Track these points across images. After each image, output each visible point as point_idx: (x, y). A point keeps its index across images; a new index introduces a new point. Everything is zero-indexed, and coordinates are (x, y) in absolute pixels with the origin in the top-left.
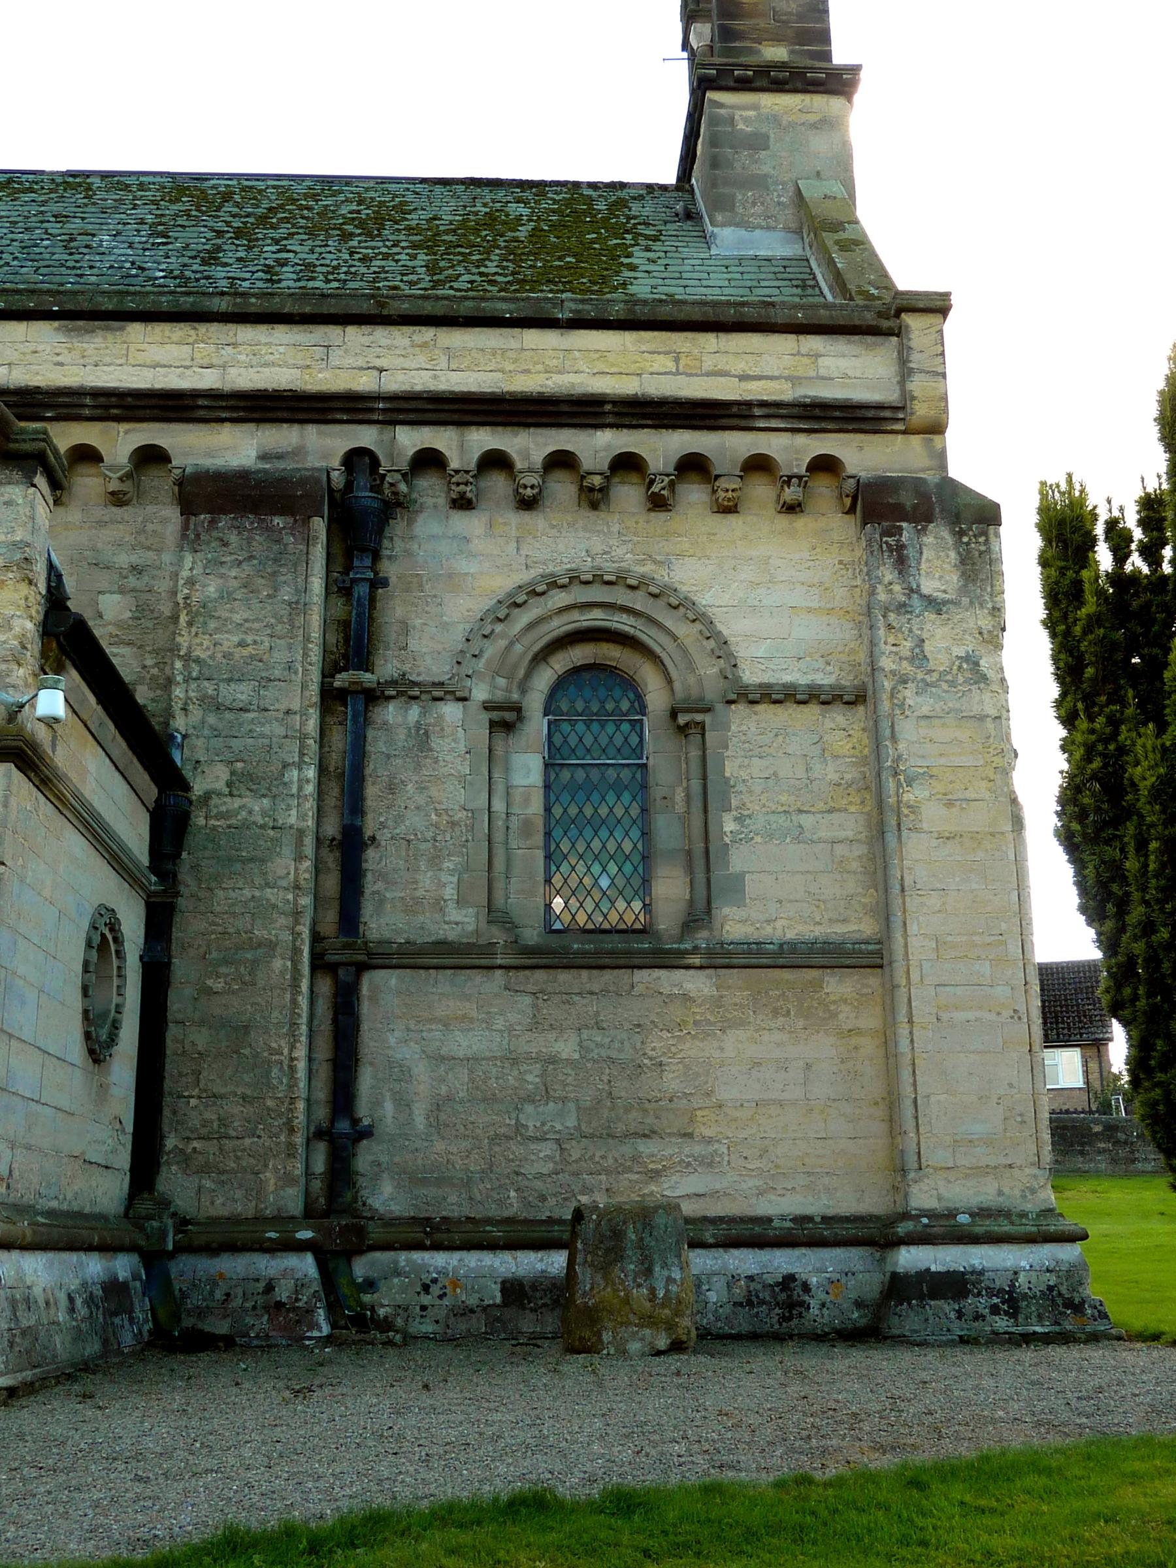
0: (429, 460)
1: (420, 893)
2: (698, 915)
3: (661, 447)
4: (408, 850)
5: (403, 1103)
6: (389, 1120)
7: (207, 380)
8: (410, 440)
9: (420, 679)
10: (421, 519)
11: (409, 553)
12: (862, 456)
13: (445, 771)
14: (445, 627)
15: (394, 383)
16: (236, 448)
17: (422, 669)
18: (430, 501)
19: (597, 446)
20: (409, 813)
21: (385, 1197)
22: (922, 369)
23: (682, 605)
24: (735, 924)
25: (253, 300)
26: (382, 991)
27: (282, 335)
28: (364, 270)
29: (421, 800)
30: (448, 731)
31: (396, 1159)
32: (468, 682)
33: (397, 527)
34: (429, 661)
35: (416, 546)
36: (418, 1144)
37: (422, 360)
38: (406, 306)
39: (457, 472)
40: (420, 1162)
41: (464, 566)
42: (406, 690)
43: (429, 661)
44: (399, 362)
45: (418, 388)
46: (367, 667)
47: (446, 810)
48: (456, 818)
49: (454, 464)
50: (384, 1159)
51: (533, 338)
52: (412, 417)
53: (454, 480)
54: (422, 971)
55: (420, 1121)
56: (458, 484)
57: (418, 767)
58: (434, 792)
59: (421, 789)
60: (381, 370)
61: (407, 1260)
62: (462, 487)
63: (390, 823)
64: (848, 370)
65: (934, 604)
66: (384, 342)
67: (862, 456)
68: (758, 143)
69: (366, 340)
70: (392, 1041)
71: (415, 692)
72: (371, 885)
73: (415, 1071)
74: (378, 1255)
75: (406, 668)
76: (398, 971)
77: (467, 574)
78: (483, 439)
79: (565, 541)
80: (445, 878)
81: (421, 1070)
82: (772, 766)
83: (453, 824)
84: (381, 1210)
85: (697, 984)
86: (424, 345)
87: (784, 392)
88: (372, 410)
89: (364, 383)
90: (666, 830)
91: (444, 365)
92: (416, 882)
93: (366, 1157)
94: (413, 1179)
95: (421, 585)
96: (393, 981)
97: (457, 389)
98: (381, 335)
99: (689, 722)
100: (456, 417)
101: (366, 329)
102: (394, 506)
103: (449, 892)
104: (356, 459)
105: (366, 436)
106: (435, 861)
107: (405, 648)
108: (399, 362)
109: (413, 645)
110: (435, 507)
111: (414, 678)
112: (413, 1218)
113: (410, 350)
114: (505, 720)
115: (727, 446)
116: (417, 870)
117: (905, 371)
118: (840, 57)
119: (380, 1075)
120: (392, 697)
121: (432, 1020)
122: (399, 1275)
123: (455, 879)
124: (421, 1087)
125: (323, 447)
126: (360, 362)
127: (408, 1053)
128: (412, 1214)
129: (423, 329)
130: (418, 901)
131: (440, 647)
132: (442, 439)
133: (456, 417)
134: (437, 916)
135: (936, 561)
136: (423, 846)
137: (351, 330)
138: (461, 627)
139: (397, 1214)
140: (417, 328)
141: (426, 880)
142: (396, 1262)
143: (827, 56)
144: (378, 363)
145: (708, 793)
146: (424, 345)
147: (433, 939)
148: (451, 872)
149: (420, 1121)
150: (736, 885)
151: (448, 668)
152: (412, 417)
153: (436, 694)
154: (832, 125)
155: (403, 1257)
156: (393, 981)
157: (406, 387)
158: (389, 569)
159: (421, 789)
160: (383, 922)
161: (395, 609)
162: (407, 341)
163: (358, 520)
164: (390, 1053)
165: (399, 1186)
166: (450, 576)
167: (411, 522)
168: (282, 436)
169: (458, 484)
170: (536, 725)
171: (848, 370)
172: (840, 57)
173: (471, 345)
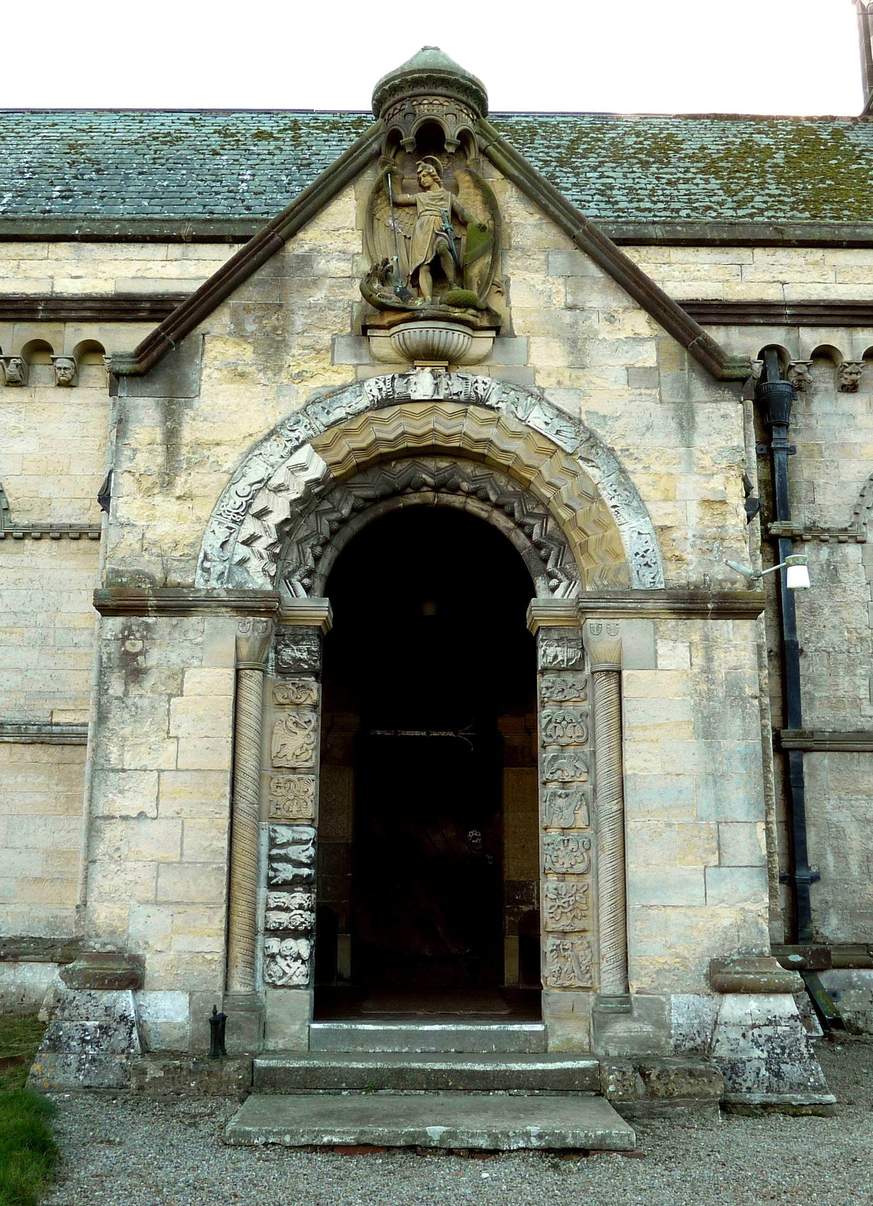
0: (825, 354)
1: (840, 693)
4: (829, 660)
5: (841, 855)
6: (832, 869)
8: (812, 338)
9: (827, 526)
10: (816, 400)
11: (809, 427)
13: (853, 598)
14: (842, 485)
15: (796, 293)
17: (827, 518)
18: (822, 386)
20: (827, 631)
25: (679, 228)
26: (819, 769)
27: (704, 255)
28: (675, 193)
29: (836, 620)
30: (852, 567)
31: (840, 898)
32: (864, 529)
33: (799, 406)
34: (833, 512)
35: (814, 422)
36: (855, 887)
37: (814, 275)
38: (798, 232)
39: (850, 364)
40: (857, 901)
41: (853, 437)
42: (818, 535)
43: (833, 512)
44: (798, 277)
45: (814, 298)
46: (787, 517)
47: (855, 629)
48: (864, 635)
49: (847, 358)
50: (829, 898)
52: (813, 320)
53: (847, 370)
54: (847, 754)
55: (855, 870)
56: (851, 374)
57: (831, 595)
58: (845, 614)
59: (835, 612)
60: (784, 283)
61: (859, 976)
62: (854, 377)
63: (813, 638)
66: (784, 261)
69: (771, 260)
70: (829, 807)
71: (826, 536)
72: (805, 687)
73: (848, 831)
74: (835, 971)
75: (816, 517)
76: (829, 753)
80: (859, 681)
81: (852, 829)
83: (862, 640)
84: (831, 937)
86: (816, 263)
88: (780, 315)
89: (772, 294)
91: (832, 279)
92: (837, 685)
93: (816, 896)
94: (852, 913)
95: (821, 453)
96: (826, 762)
97: (844, 298)
98: (782, 255)
100: (847, 321)
101: (770, 251)
103: (863, 693)
104: (772, 353)
105: (777, 336)
106: (850, 668)
107: (813, 502)
108: (798, 277)
109: (819, 499)
110: (826, 390)
111: (822, 525)
112: (855, 944)
113: (805, 267)
116: (837, 675)
119: (822, 834)
120: (808, 541)
121: (858, 792)
122: (854, 988)
123: (867, 683)
124: (854, 843)
126: (768, 277)
127: (842, 817)
128: (854, 941)
129: (814, 250)
130: (840, 700)
131: (840, 501)
133: (847, 321)
134: (856, 711)
136: (840, 657)
137: (758, 251)
138: (854, 485)
139: (843, 940)
140: (809, 250)
141: (845, 683)
142: (850, 978)
144: (781, 278)
146: (816, 263)
147: (854, 728)
148: (864, 677)
149: (855, 870)
151: (847, 518)
152: (813, 320)
153: (842, 538)
155: (855, 974)
156: (826, 762)
157: (805, 297)
158: (797, 440)
159: (835, 612)
160: (815, 716)
161: (803, 471)
162: (802, 261)
164: (828, 816)
165: (843, 919)
166: (843, 445)
167: (808, 403)
169: (851, 374)
173: (852, 263)
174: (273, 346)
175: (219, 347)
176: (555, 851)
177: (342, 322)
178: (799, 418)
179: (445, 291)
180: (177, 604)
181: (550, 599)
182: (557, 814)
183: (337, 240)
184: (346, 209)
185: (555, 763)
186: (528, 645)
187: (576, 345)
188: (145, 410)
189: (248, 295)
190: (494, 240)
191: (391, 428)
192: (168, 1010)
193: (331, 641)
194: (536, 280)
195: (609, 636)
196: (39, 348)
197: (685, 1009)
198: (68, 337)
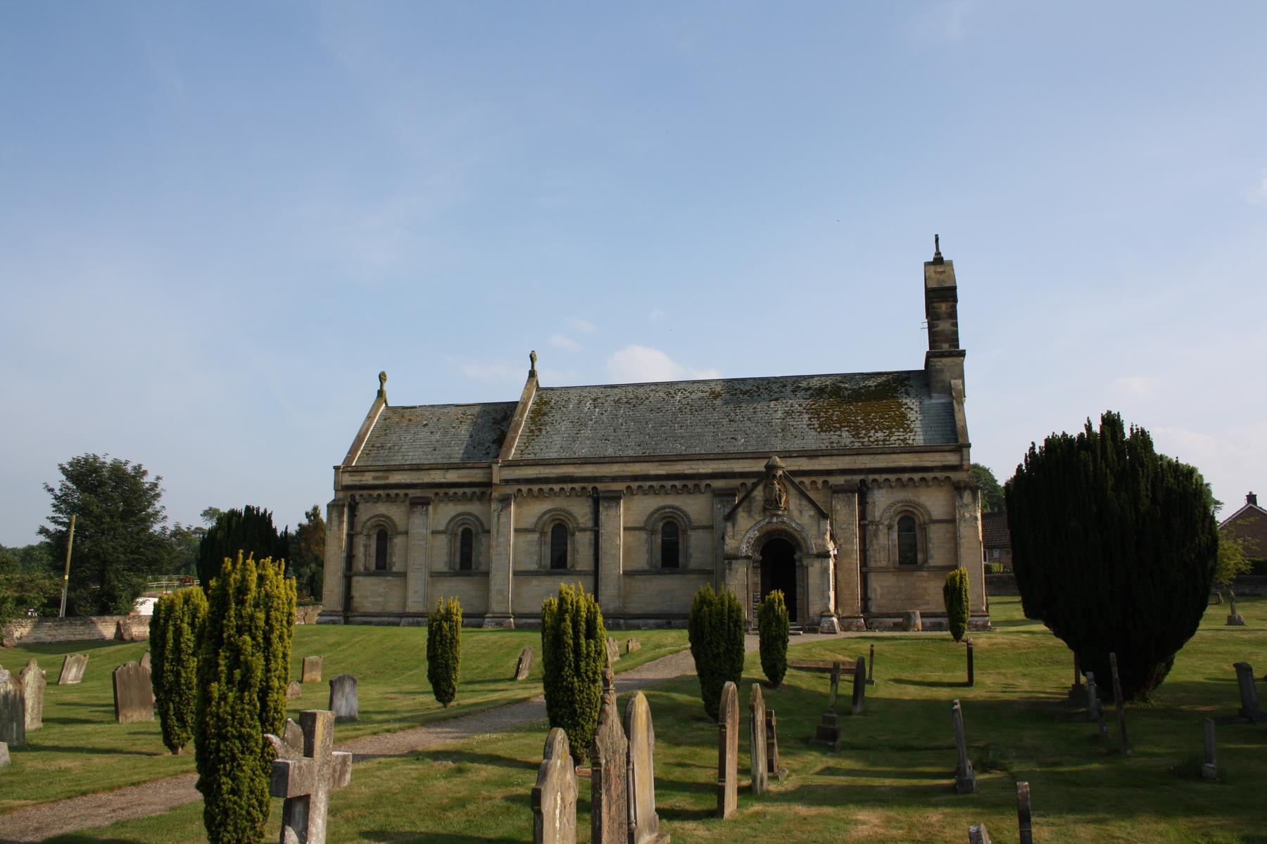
2: (926, 561)
7: (834, 467)
8: (871, 477)
12: (955, 476)
15: (868, 466)
16: (839, 480)
19: (905, 477)
21: (873, 609)
23: (922, 506)
24: (932, 562)
42: (872, 522)
51: (893, 456)
65: (966, 505)
68: (942, 371)
77: (882, 501)
78: (885, 476)
79: (901, 495)
82: (936, 535)
85: (925, 574)
87: (939, 464)
90: (919, 546)
102: (869, 489)
104: (862, 481)
105: (862, 477)
114: (890, 527)
118: (961, 348)
125: (858, 478)
132: (877, 477)
143: (957, 346)
150: (932, 557)
161: (869, 507)
163: (863, 491)
168: (849, 478)
170: (896, 527)
172: (961, 348)
174: (749, 512)
176: (799, 596)
177: (760, 508)
178: (869, 494)
180: (736, 558)
182: (799, 590)
184: (760, 488)
188: (729, 524)
189: (745, 504)
191: (770, 527)
196: (696, 486)
198: (703, 483)
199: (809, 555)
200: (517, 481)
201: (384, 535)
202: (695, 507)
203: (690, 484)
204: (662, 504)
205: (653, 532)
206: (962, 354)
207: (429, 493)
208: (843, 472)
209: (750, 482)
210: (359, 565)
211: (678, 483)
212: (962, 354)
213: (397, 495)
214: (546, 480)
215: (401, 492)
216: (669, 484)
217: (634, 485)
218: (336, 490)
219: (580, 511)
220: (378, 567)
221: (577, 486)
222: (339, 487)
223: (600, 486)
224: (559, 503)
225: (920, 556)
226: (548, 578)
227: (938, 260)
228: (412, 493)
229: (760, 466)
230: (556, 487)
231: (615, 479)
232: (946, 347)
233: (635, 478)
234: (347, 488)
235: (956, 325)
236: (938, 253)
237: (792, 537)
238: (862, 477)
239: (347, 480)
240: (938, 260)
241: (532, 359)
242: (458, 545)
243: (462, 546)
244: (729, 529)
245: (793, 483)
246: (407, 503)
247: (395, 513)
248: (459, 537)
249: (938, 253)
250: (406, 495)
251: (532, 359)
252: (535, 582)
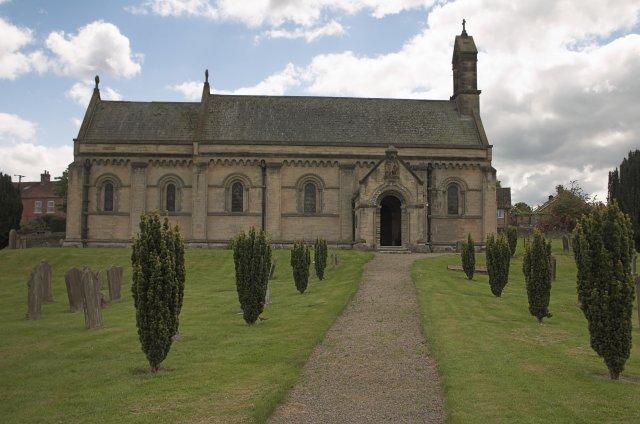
2: (464, 212)
3: (461, 163)
12: (483, 164)
16: (416, 163)
22: (489, 154)
64: (482, 154)
67: (483, 164)
77: (441, 177)
79: (451, 174)
82: (471, 197)
99: (463, 193)
105: (429, 162)
114: (444, 192)
115: (468, 163)
117: (487, 154)
125: (427, 162)
135: (490, 176)
145: (464, 200)
154: (478, 99)
163: (429, 171)
171: (482, 154)
175: (370, 179)
176: (403, 230)
178: (433, 173)
179: (392, 176)
180: (367, 207)
181: (403, 206)
182: (403, 227)
183: (382, 168)
184: (383, 164)
185: (403, 223)
186: (400, 210)
187: (407, 179)
189: (373, 174)
190: (398, 169)
192: (368, 245)
193: (381, 209)
194: (403, 173)
195: (409, 210)
197: (415, 244)
198: (333, 161)
199: (410, 206)
200: (210, 154)
201: (110, 187)
202: (330, 176)
203: (325, 160)
204: (307, 172)
205: (301, 190)
206: (479, 92)
207: (146, 160)
208: (419, 158)
209: (376, 161)
210: (93, 208)
211: (318, 160)
212: (479, 92)
213: (122, 160)
214: (231, 154)
215: (125, 159)
216: (311, 160)
217: (289, 160)
218: (75, 156)
219: (254, 175)
220: (106, 209)
221: (252, 159)
222: (77, 154)
223: (268, 160)
224: (239, 169)
225: (460, 210)
226: (231, 218)
227: (464, 33)
228: (133, 159)
229: (381, 152)
230: (237, 159)
231: (277, 155)
232: (470, 87)
233: (290, 155)
234: (84, 154)
235: (475, 75)
236: (464, 31)
237: (400, 194)
238: (429, 162)
239: (84, 148)
240: (464, 33)
241: (207, 75)
242: (165, 194)
243: (168, 196)
244: (363, 188)
245: (403, 163)
246: (129, 166)
247: (123, 174)
248: (166, 191)
249: (464, 31)
250: (128, 160)
251: (207, 75)
252: (222, 220)
